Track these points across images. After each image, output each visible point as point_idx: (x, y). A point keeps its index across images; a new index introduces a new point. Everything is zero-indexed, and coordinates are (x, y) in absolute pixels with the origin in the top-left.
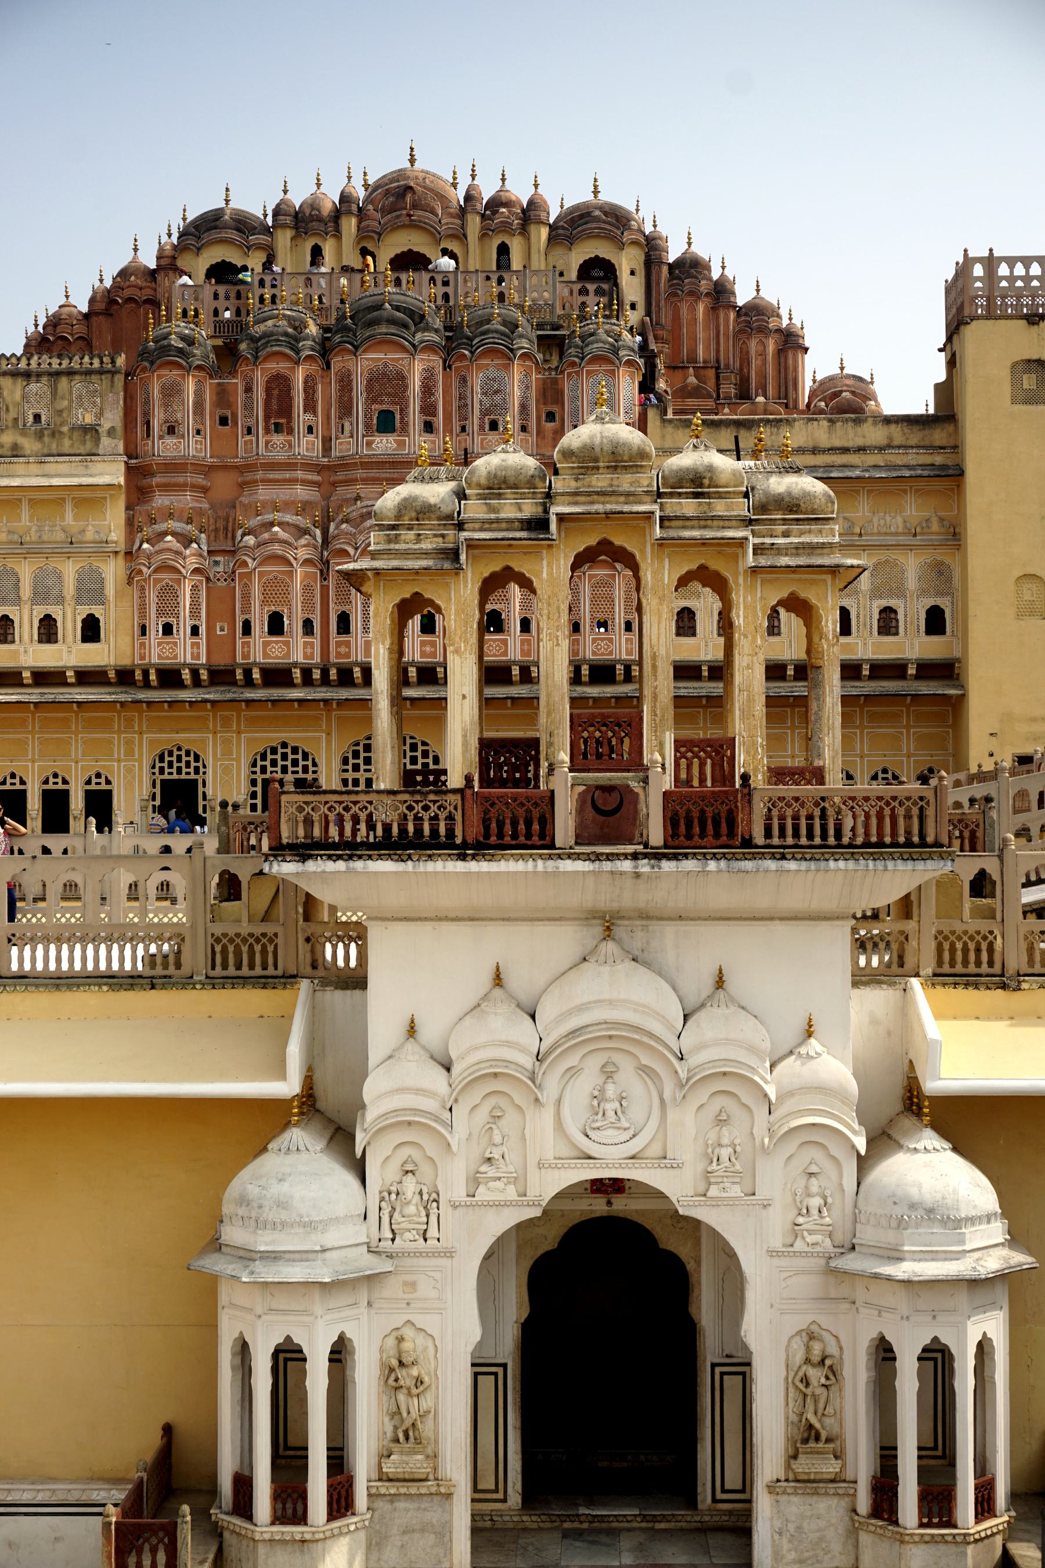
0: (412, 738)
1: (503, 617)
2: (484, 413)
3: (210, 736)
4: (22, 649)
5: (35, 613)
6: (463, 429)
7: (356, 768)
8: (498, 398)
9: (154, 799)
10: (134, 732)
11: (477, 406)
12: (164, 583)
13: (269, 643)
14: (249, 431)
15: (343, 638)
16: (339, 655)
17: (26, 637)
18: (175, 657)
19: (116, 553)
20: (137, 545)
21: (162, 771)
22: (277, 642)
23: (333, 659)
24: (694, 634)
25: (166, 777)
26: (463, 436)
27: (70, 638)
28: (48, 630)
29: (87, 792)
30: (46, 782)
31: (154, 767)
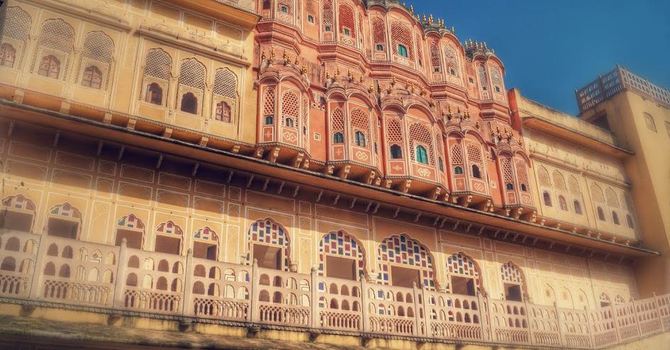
0: (415, 243)
1: (480, 170)
2: (448, 65)
3: (294, 216)
4: (167, 112)
5: (181, 88)
6: (437, 70)
7: (385, 259)
8: (453, 60)
9: (248, 259)
10: (238, 202)
11: (445, 61)
12: (288, 91)
13: (357, 150)
14: (328, 28)
15: (396, 161)
16: (394, 171)
17: (172, 103)
18: (295, 143)
19: (247, 66)
20: (264, 64)
21: (255, 237)
22: (362, 151)
23: (389, 173)
24: (551, 206)
25: (258, 242)
26: (437, 74)
27: (208, 115)
28: (189, 104)
29: (196, 243)
30: (161, 229)
31: (249, 234)
